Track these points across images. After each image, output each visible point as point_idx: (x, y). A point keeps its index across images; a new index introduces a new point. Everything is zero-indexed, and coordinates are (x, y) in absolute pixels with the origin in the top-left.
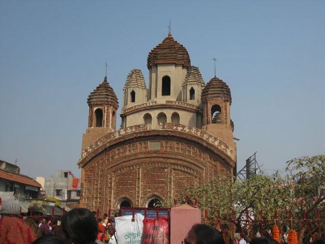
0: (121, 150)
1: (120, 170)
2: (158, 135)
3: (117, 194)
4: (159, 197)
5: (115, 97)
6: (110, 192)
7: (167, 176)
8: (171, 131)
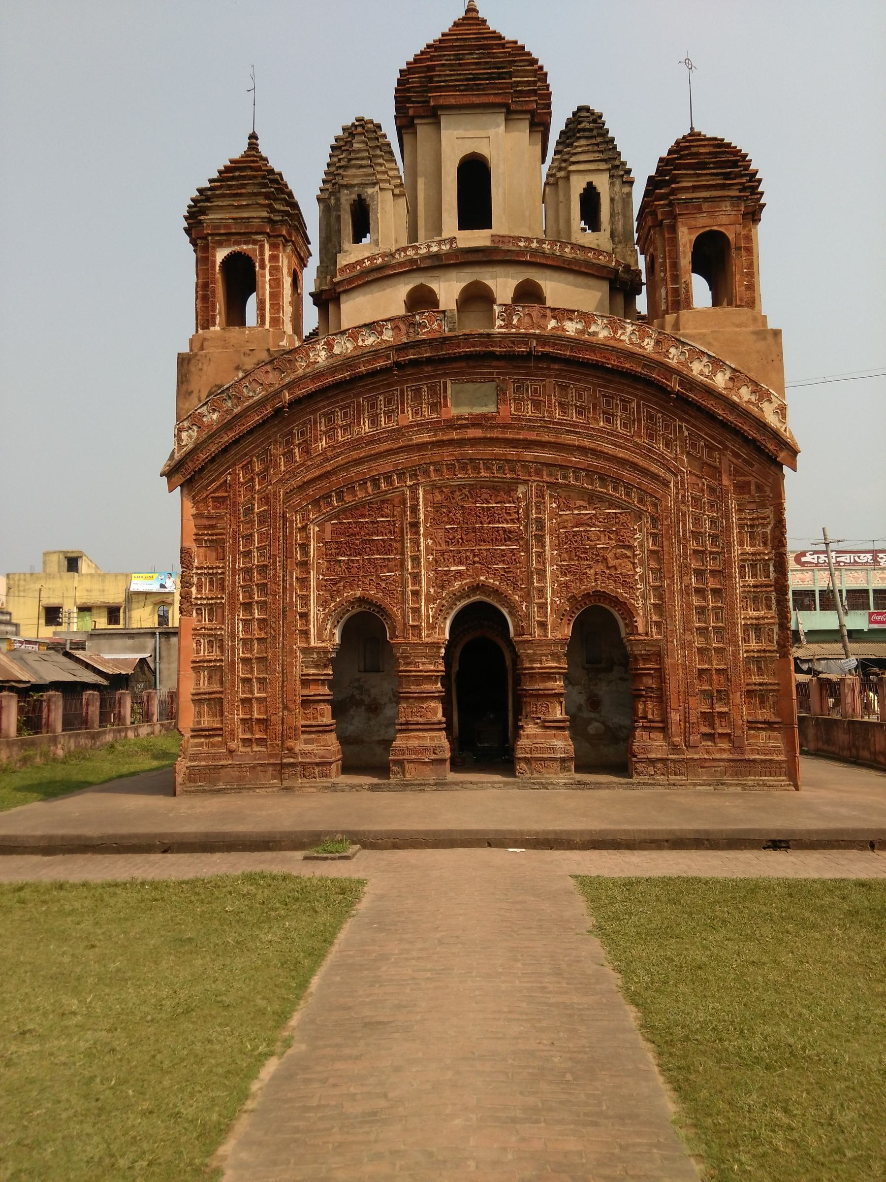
2: (492, 356)
4: (496, 592)
5: (295, 206)
6: (304, 582)
7: (527, 516)
8: (537, 337)
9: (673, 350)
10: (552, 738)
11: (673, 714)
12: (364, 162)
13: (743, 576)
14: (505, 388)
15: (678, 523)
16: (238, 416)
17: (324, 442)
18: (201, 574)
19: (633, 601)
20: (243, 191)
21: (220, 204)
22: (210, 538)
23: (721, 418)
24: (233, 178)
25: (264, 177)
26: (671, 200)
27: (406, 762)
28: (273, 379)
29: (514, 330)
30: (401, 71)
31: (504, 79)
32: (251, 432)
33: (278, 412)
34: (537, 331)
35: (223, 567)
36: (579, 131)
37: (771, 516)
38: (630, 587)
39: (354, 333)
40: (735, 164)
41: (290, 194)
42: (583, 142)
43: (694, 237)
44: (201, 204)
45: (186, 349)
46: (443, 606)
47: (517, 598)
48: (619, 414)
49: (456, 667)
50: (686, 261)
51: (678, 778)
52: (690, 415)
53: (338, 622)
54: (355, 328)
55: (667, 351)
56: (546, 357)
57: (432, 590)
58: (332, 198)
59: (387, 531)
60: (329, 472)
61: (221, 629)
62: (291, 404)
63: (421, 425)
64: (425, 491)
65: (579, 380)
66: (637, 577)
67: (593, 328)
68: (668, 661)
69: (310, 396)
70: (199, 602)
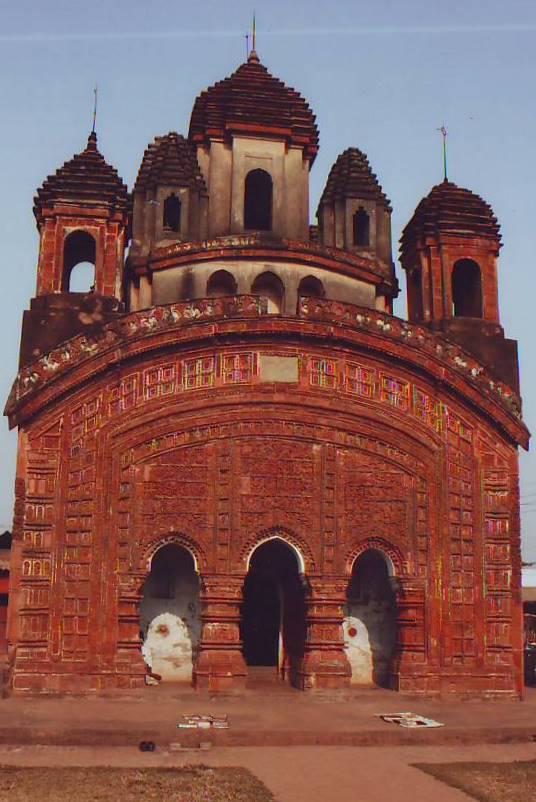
0: (161, 375)
33: (111, 367)
43: (452, 263)
65: (365, 363)
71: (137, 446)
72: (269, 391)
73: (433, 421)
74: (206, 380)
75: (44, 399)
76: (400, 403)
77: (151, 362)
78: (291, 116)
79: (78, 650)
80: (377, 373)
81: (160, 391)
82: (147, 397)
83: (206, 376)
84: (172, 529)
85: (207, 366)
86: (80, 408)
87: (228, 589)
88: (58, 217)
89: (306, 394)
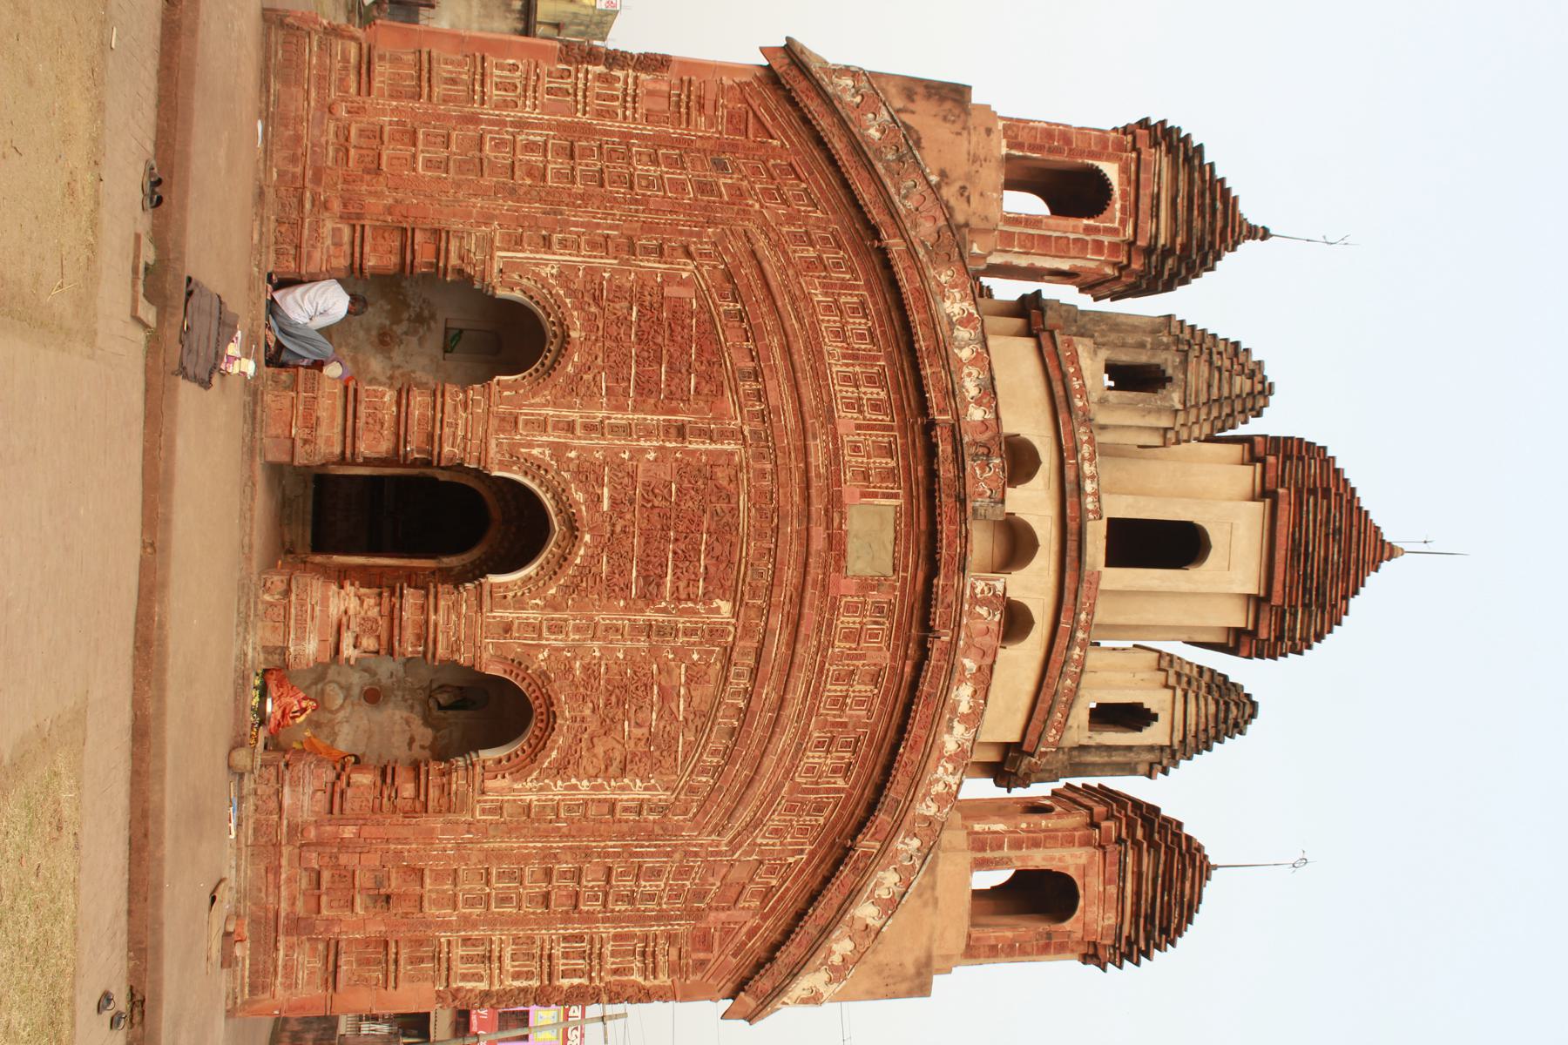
0: (858, 324)
1: (741, 316)
2: (933, 571)
3: (593, 292)
5: (1169, 287)
8: (954, 643)
9: (916, 843)
10: (320, 633)
11: (353, 829)
12: (1215, 390)
13: (566, 939)
14: (882, 589)
15: (655, 846)
16: (870, 168)
17: (820, 298)
18: (626, 83)
19: (535, 774)
20: (1196, 213)
21: (1181, 177)
22: (683, 105)
23: (810, 911)
24: (1213, 200)
25: (1212, 245)
26: (1125, 841)
27: (294, 394)
28: (925, 230)
29: (966, 607)
30: (1324, 448)
31: (1304, 596)
32: (846, 185)
33: (874, 231)
34: (961, 643)
35: (634, 119)
36: (1227, 704)
37: (657, 982)
38: (561, 769)
39: (984, 359)
40: (1165, 930)
41: (1185, 282)
42: (1212, 708)
43: (1071, 872)
44: (1182, 149)
45: (976, 98)
46: (546, 471)
47: (553, 591)
48: (829, 761)
49: (443, 476)
50: (1038, 859)
51: (250, 832)
52: (818, 867)
53: (531, 298)
54: (990, 363)
55: (915, 835)
56: (924, 653)
57: (573, 454)
58: (1171, 339)
59: (673, 388)
60: (774, 302)
61: (535, 106)
62: (883, 252)
63: (836, 455)
64: (732, 454)
66: (574, 781)
67: (959, 729)
68: (437, 823)
69: (894, 284)
70: (581, 75)
71: (729, 276)
72: (829, 521)
73: (776, 831)
74: (849, 406)
75: (813, 106)
76: (811, 770)
77: (881, 305)
78: (1304, 605)
79: (352, 152)
80: (866, 725)
81: (828, 322)
82: (819, 297)
83: (855, 405)
84: (574, 334)
85: (876, 407)
86: (798, 177)
87: (460, 433)
88: (1134, 155)
89: (825, 587)
